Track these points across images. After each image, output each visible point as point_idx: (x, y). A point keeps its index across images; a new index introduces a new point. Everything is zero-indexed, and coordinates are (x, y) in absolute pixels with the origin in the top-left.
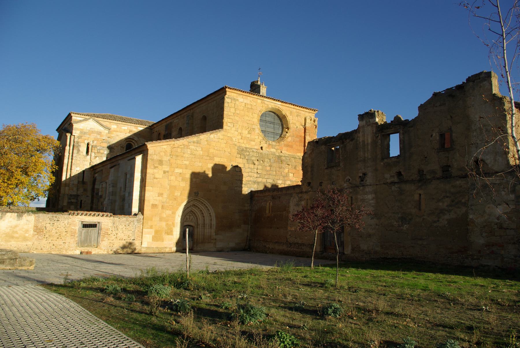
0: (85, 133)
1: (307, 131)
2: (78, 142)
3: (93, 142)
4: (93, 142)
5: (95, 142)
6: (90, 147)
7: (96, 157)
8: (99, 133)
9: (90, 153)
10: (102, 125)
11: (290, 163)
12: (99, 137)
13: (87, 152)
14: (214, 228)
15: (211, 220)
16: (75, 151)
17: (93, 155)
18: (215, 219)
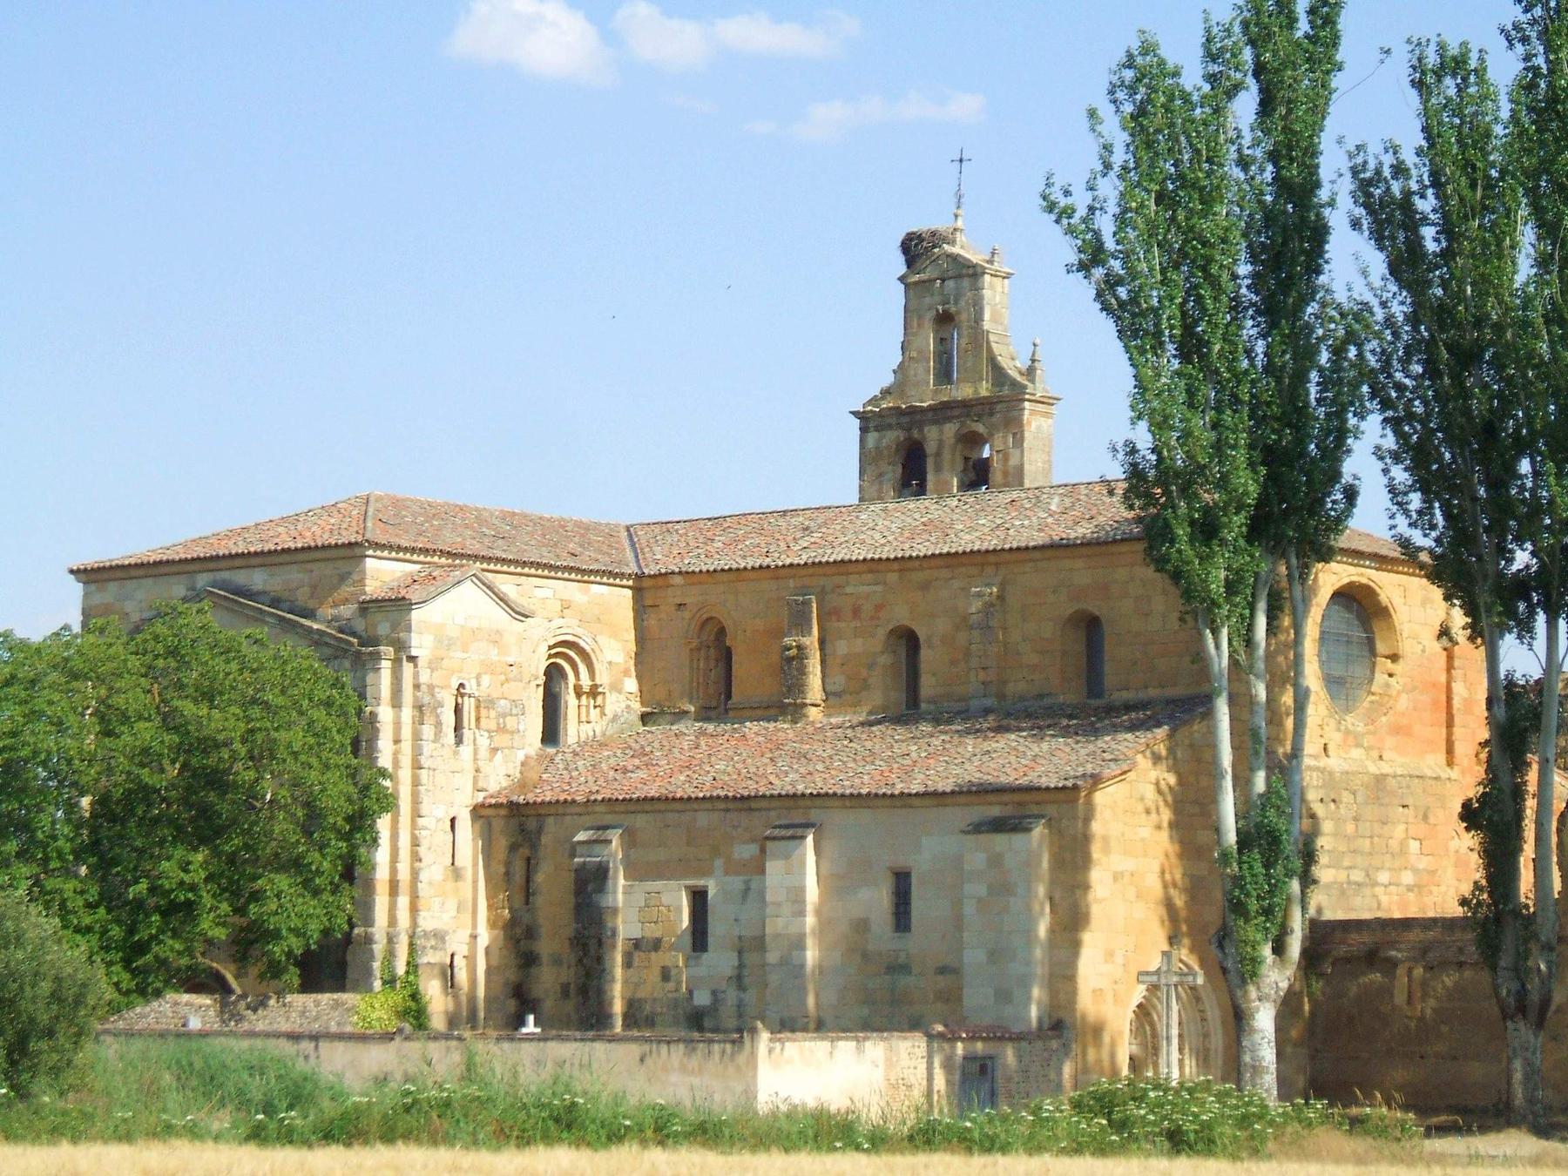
0: (451, 644)
1: (1457, 663)
2: (431, 687)
3: (478, 678)
4: (478, 678)
5: (486, 680)
6: (468, 705)
7: (494, 750)
8: (496, 638)
9: (467, 734)
10: (502, 599)
11: (1409, 801)
12: (494, 654)
13: (458, 728)
14: (1220, 1062)
15: (1206, 1036)
16: (428, 731)
17: (484, 741)
18: (1220, 1031)
